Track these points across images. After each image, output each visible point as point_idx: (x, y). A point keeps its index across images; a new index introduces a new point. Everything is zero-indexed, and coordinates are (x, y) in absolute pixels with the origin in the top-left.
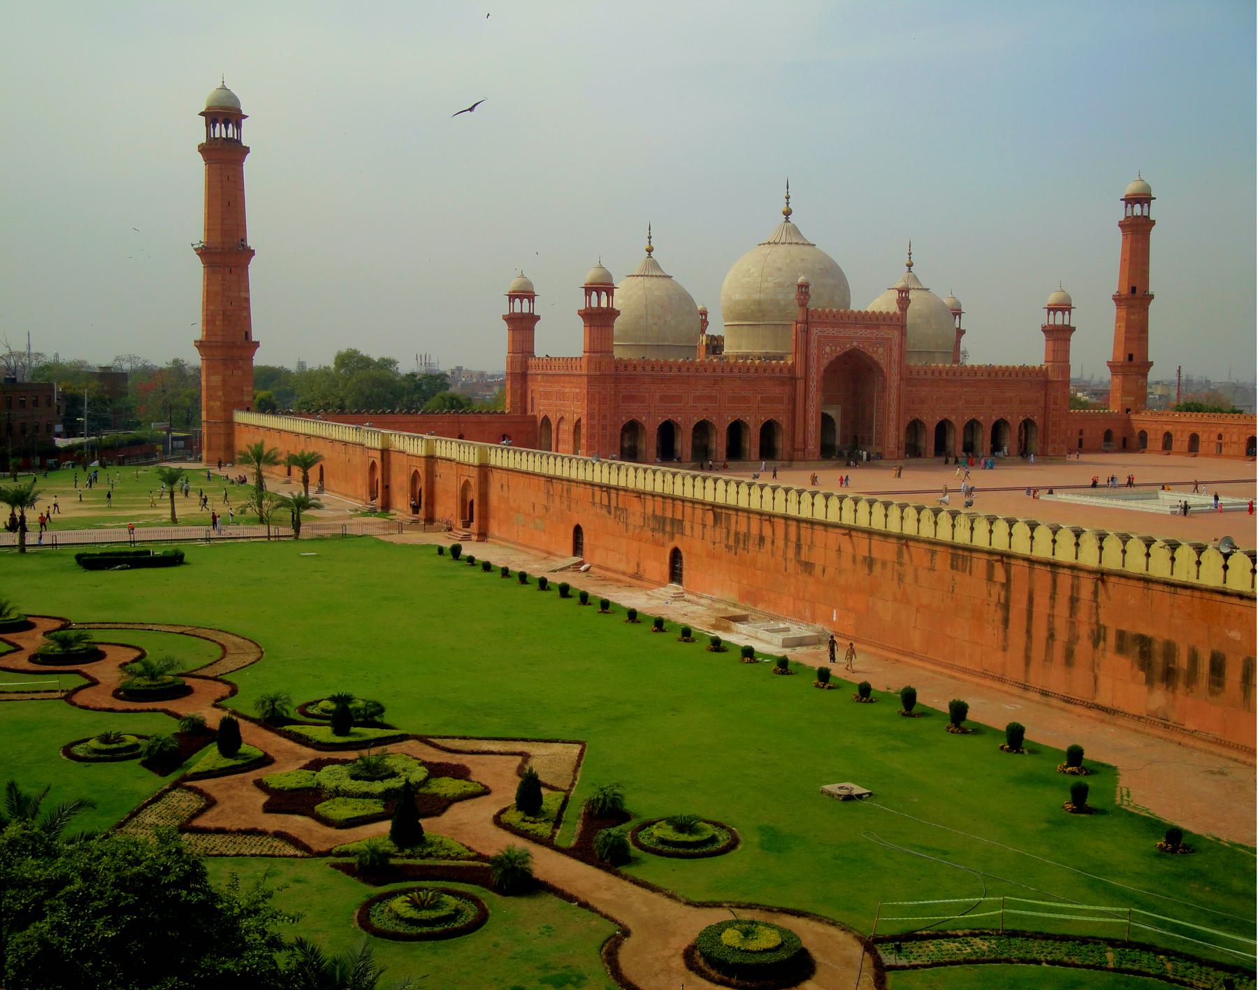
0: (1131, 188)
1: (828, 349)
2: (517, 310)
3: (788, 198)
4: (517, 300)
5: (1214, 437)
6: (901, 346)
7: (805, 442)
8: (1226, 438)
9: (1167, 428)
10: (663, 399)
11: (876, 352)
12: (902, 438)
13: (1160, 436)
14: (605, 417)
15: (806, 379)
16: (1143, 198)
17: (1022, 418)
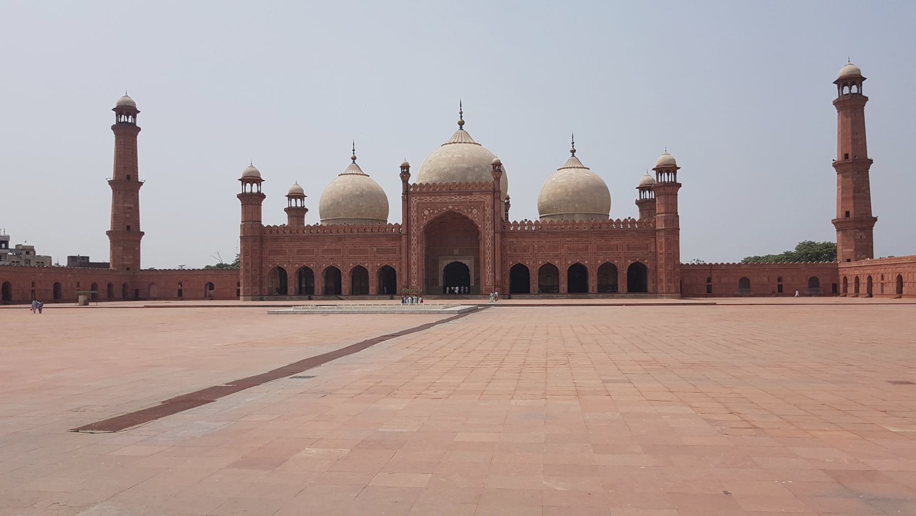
0: (842, 70)
1: (426, 212)
2: (293, 205)
3: (461, 113)
4: (293, 200)
5: (879, 277)
6: (493, 207)
7: (408, 281)
8: (886, 277)
9: (857, 272)
10: (299, 252)
11: (471, 212)
12: (498, 277)
13: (853, 281)
14: (247, 264)
15: (408, 234)
16: (854, 79)
17: (630, 262)
